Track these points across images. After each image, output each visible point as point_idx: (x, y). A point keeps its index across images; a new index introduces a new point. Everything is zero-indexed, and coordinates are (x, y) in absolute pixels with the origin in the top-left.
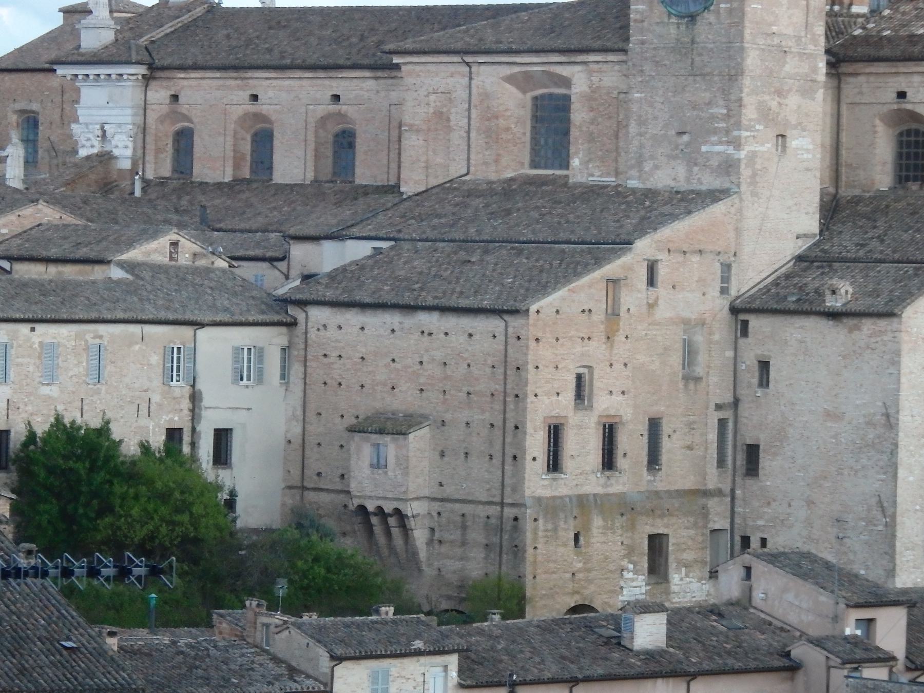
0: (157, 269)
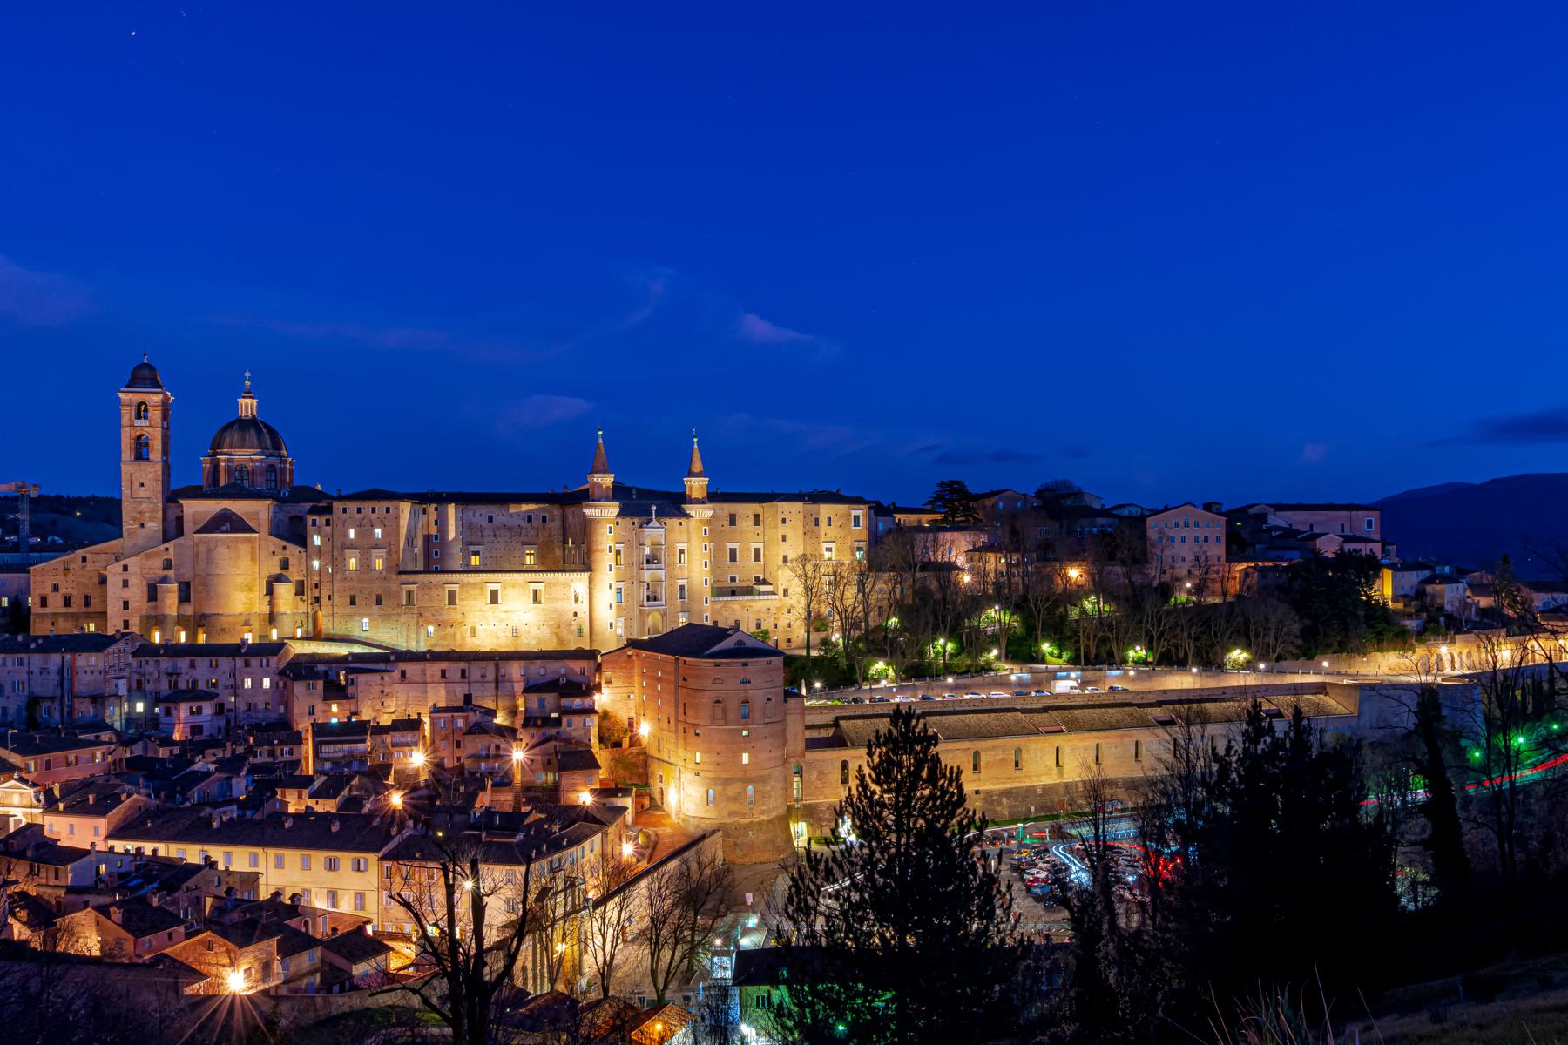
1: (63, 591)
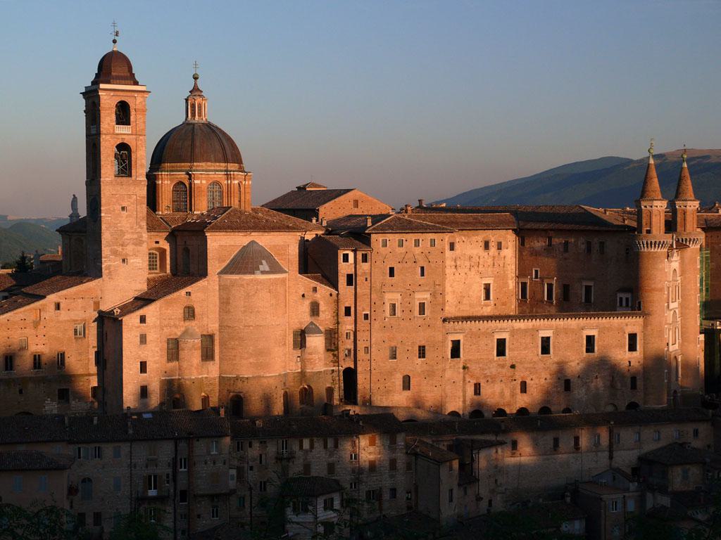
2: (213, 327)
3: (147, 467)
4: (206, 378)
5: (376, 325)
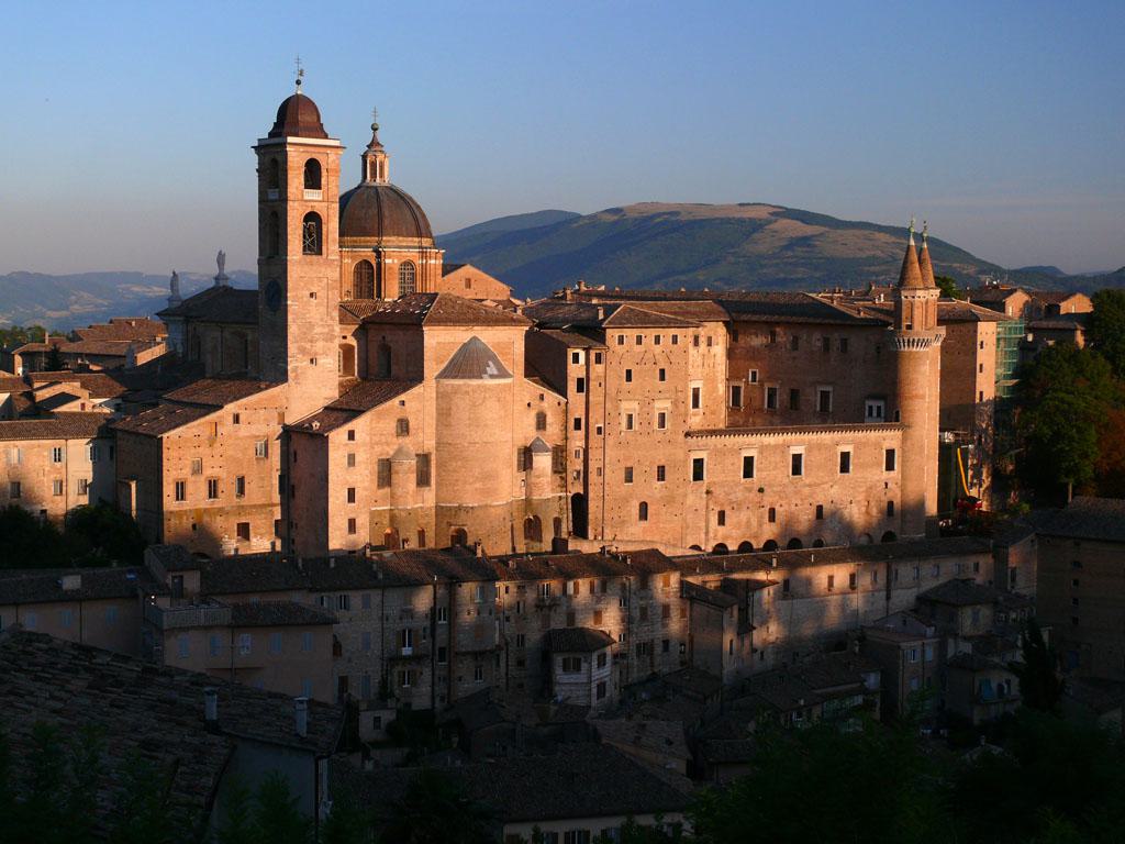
0: (74, 414)
1: (208, 472)
2: (429, 444)
3: (401, 619)
4: (422, 508)
5: (610, 441)
